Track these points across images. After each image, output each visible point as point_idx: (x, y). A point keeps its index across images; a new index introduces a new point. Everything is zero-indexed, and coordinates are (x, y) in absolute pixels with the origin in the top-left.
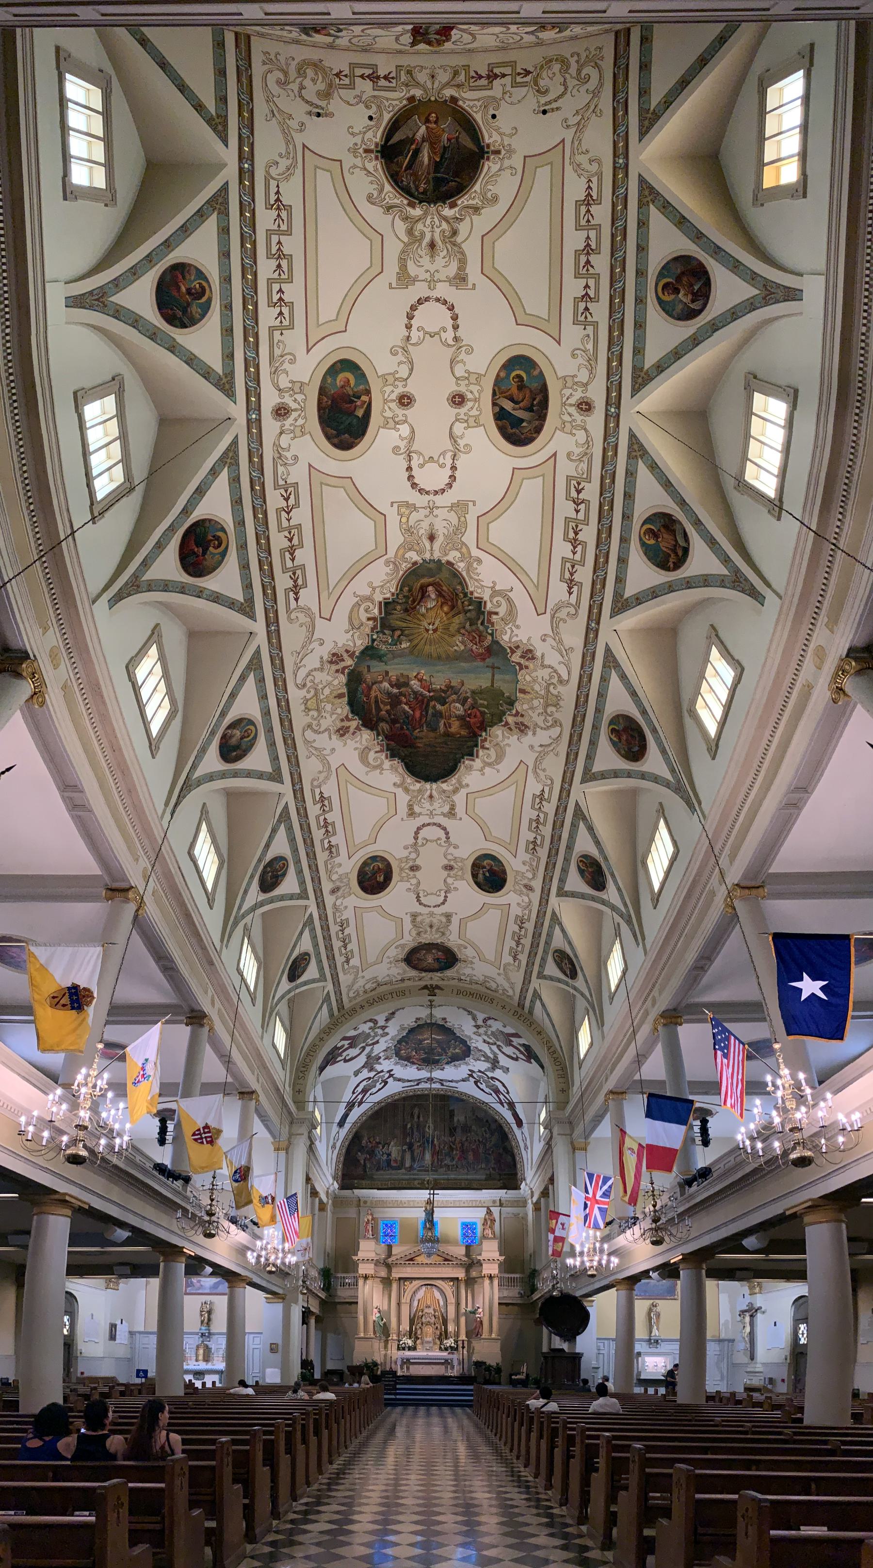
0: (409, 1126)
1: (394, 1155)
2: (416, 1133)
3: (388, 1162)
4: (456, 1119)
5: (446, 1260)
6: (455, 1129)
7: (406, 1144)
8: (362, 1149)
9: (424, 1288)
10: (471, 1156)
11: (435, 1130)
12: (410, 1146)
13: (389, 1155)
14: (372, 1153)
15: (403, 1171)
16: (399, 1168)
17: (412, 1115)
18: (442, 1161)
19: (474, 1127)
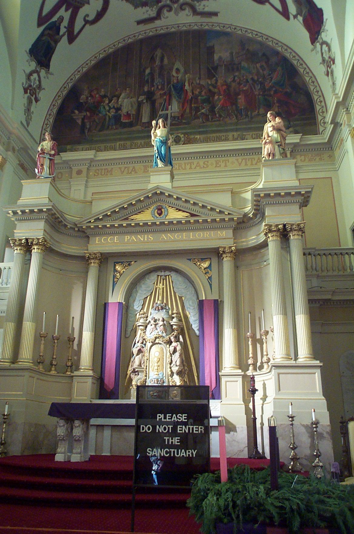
0: (148, 71)
1: (124, 111)
2: (157, 81)
3: (117, 118)
4: (216, 57)
5: (192, 215)
6: (215, 68)
7: (144, 93)
8: (80, 107)
9: (153, 277)
10: (241, 100)
11: (186, 72)
12: (150, 96)
13: (118, 109)
14: (94, 109)
15: (139, 128)
16: (131, 125)
17: (153, 59)
18: (197, 109)
19: (244, 64)
